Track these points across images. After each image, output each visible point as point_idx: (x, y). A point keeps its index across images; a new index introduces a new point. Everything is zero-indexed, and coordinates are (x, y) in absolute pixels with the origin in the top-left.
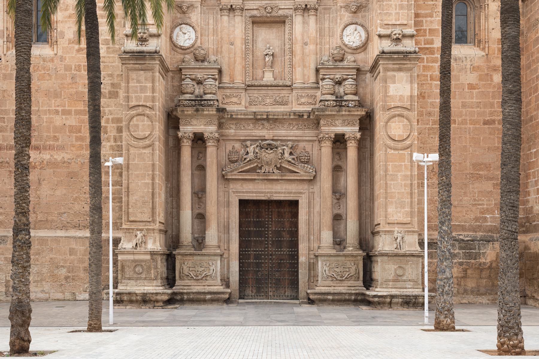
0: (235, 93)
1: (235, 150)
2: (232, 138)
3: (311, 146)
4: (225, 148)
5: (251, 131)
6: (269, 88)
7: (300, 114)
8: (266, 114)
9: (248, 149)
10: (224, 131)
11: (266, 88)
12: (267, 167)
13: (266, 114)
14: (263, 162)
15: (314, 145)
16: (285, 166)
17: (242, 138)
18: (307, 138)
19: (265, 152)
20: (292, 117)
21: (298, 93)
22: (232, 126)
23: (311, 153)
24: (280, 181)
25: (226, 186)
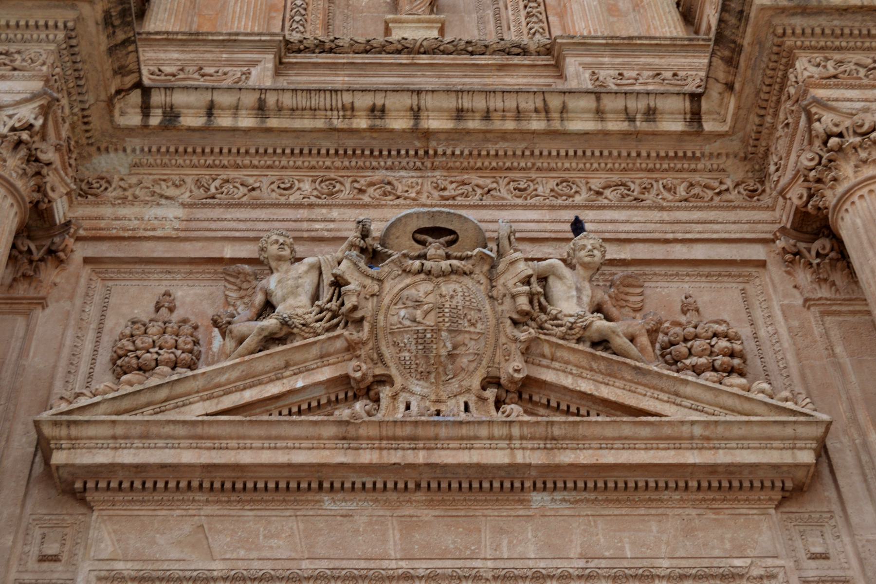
0: (214, 63)
1: (175, 317)
2: (160, 250)
3: (736, 295)
4: (105, 308)
5: (303, 213)
6: (424, 59)
7: (632, 104)
8: (407, 101)
9: (272, 282)
10: (107, 211)
11: (404, 59)
12: (418, 387)
13: (407, 101)
14: (388, 352)
15: (751, 289)
16: (568, 381)
17: (229, 251)
18: (699, 252)
19: (406, 272)
20: (575, 125)
21: (601, 66)
22: (171, 192)
23: (745, 331)
24: (538, 499)
25: (52, 549)
